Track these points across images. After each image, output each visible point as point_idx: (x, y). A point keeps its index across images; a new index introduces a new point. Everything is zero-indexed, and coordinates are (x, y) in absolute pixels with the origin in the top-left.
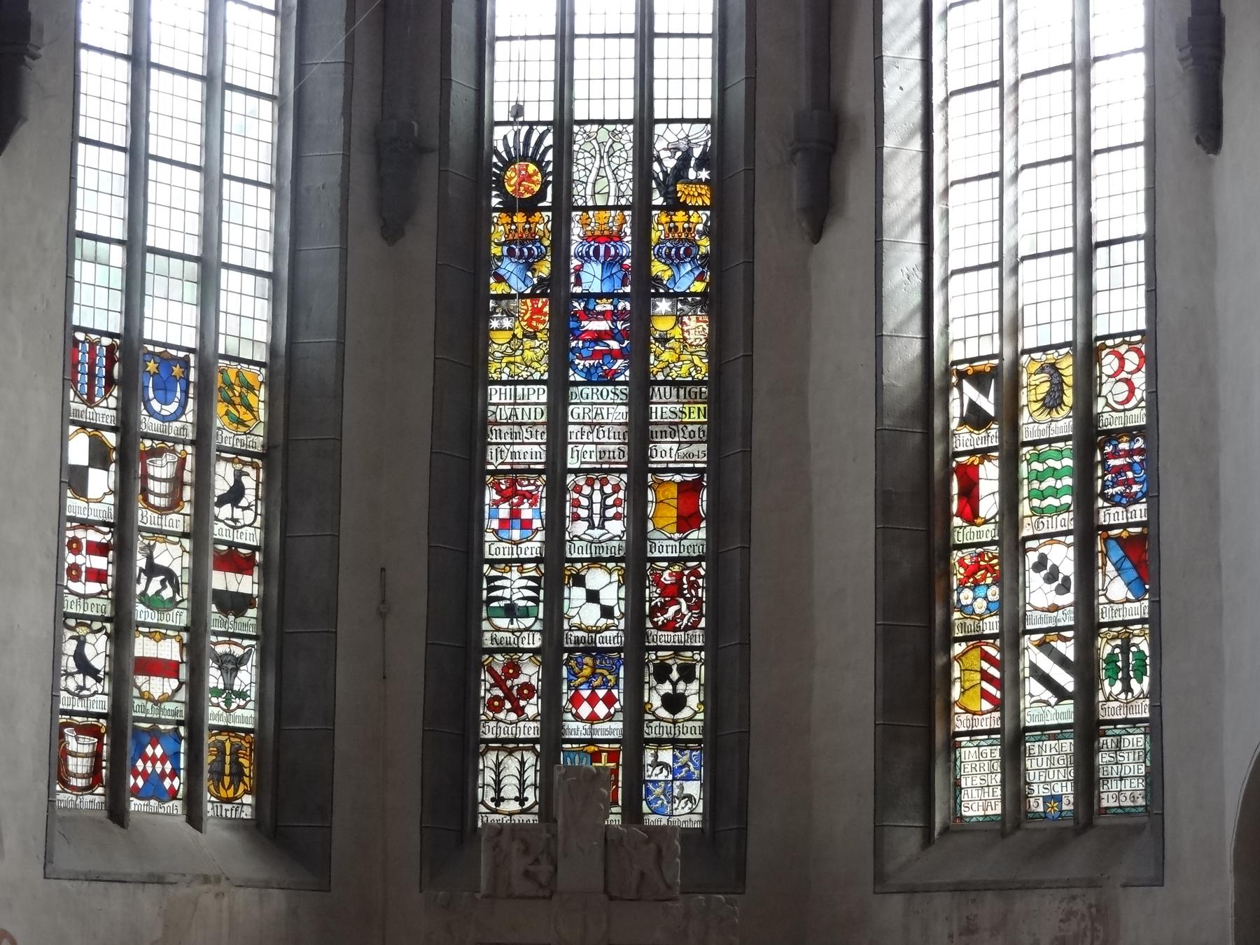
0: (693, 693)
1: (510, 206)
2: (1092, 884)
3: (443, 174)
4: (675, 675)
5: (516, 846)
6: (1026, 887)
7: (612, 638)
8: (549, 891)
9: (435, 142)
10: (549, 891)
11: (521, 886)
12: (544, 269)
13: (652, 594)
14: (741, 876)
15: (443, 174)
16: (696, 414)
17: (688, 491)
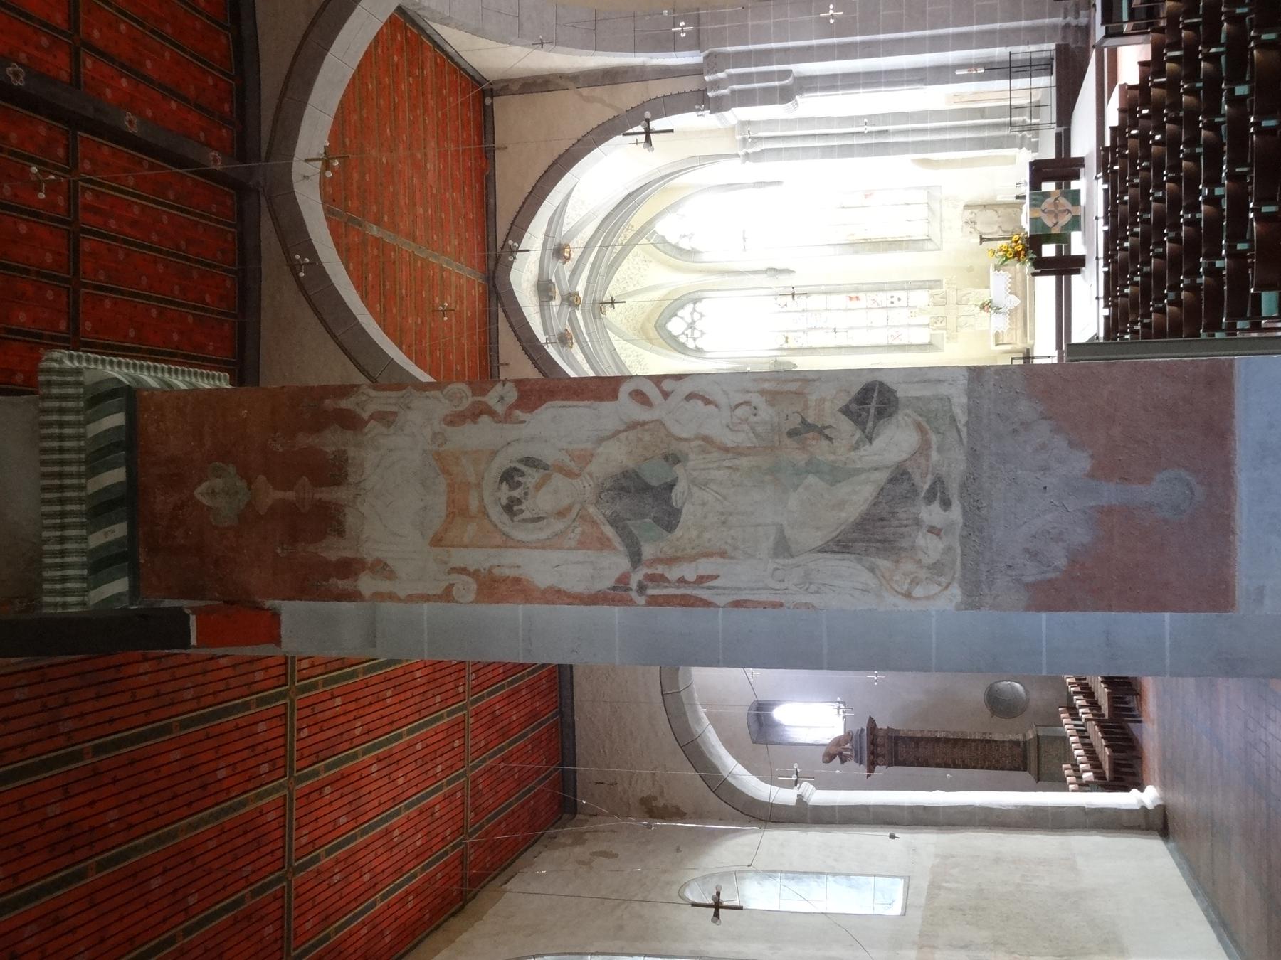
0: (897, 294)
1: (787, 342)
2: (941, 201)
3: (781, 356)
4: (892, 300)
5: (935, 325)
6: (941, 215)
7: (884, 311)
8: (945, 317)
9: (774, 359)
10: (945, 317)
11: (944, 324)
12: (801, 334)
13: (875, 305)
14: (939, 281)
15: (781, 356)
16: (834, 297)
17: (851, 298)
